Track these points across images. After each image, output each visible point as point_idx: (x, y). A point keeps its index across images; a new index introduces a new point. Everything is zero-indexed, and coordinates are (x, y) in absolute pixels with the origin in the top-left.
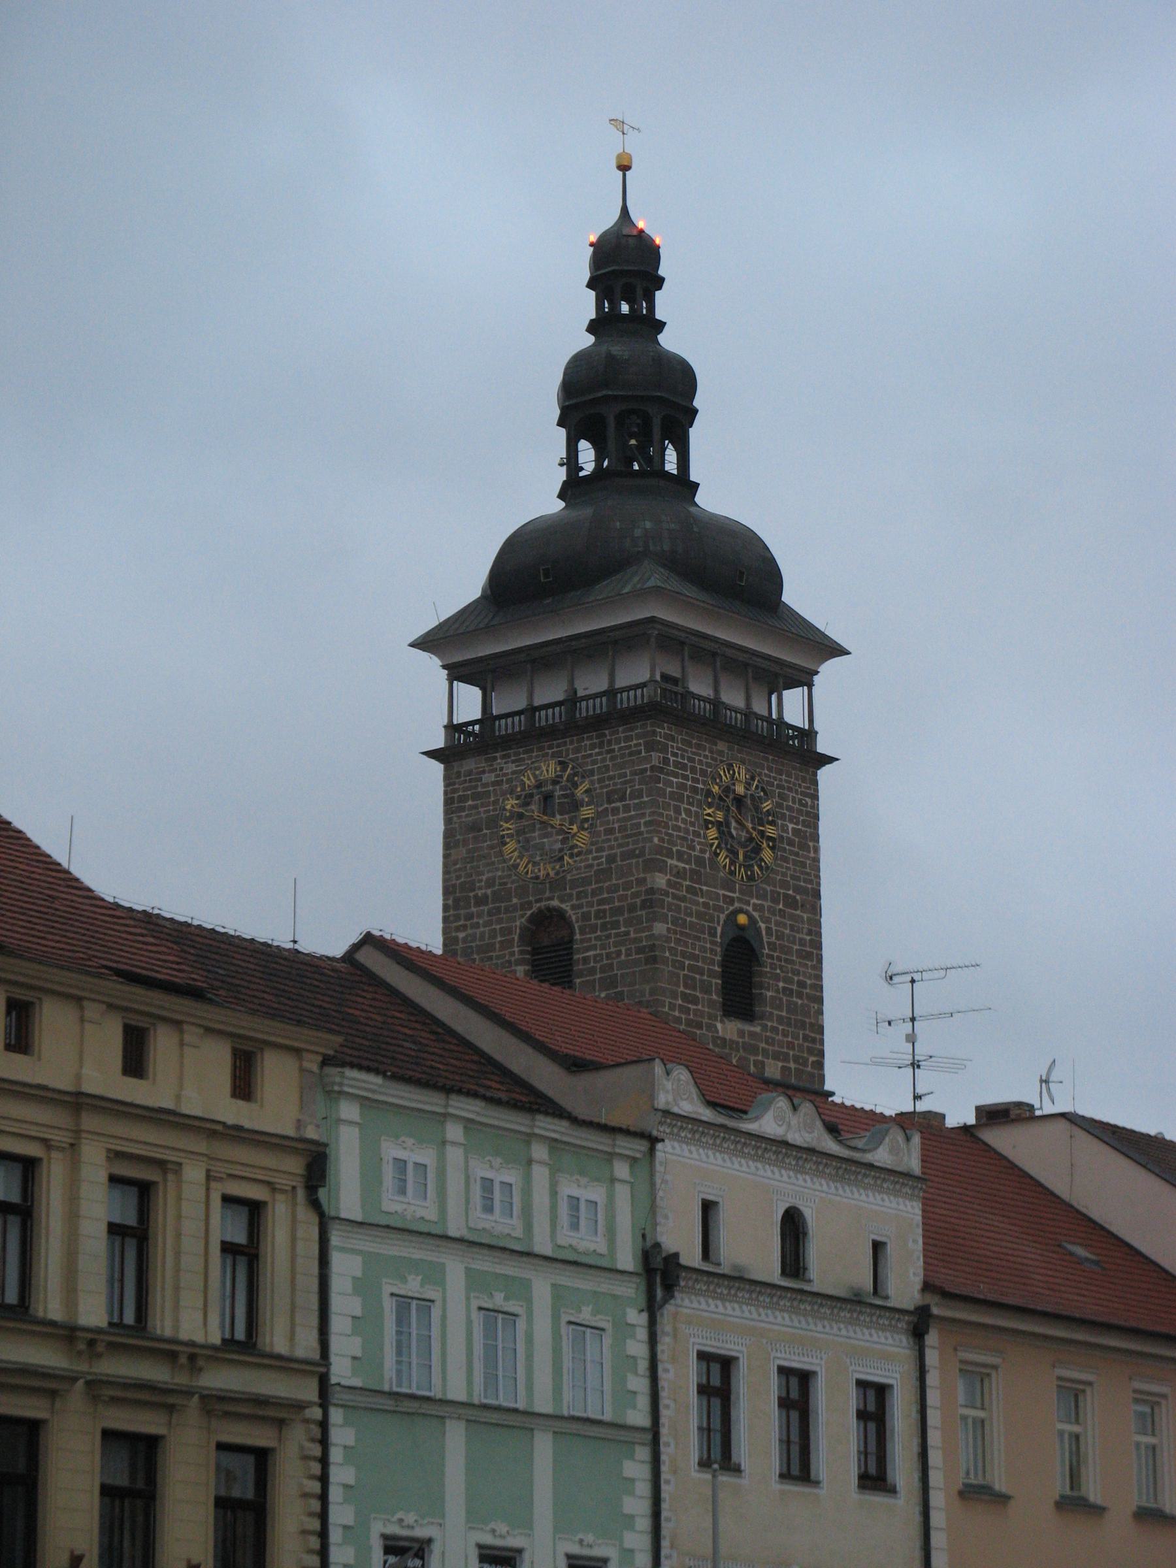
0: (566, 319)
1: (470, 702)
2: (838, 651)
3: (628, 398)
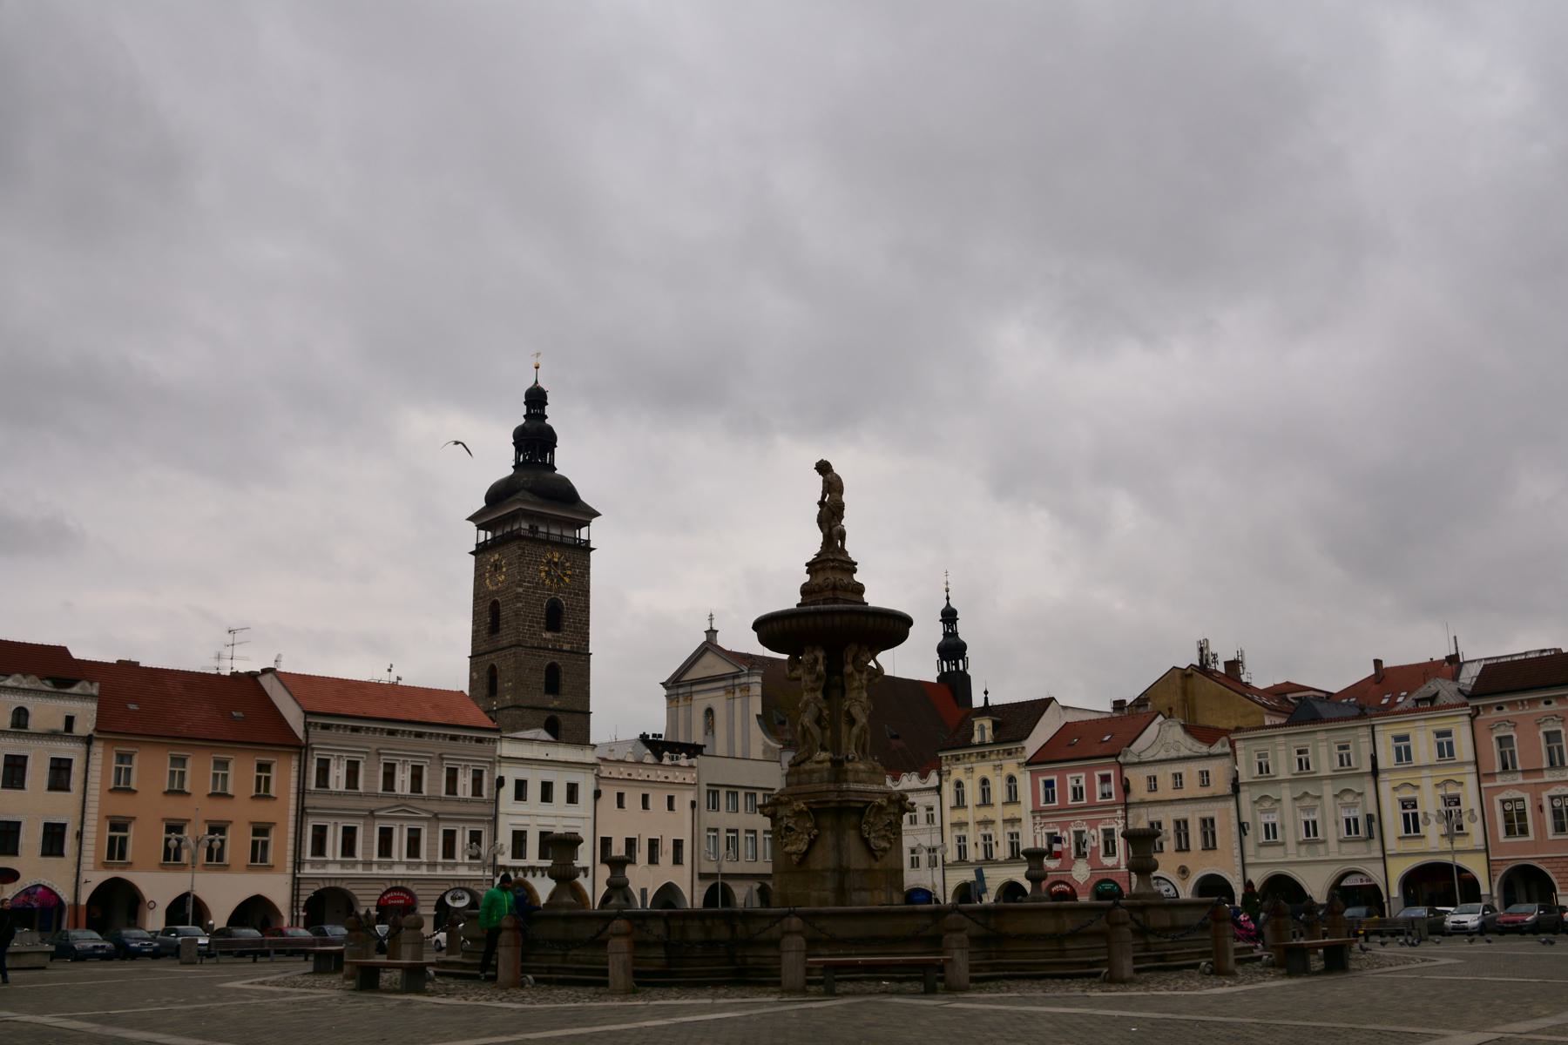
0: (517, 416)
1: (484, 536)
2: (598, 514)
3: (535, 440)
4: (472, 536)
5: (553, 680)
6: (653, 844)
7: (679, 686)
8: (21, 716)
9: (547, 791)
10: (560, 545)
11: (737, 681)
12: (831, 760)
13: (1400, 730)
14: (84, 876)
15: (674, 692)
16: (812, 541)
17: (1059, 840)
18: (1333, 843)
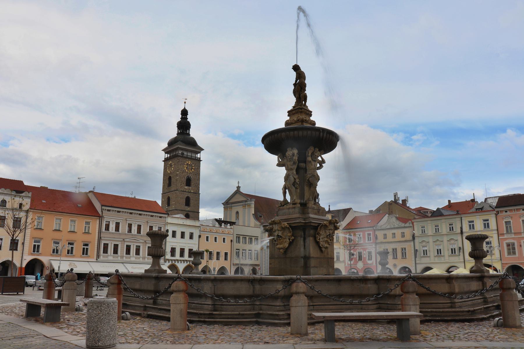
0: (178, 118)
2: (203, 150)
3: (184, 125)
4: (163, 156)
5: (188, 202)
6: (218, 253)
7: (228, 204)
8: (4, 202)
9: (183, 235)
10: (191, 159)
11: (246, 203)
12: (300, 203)
13: (471, 219)
14: (24, 257)
15: (226, 206)
16: (291, 101)
17: (353, 255)
18: (447, 257)
